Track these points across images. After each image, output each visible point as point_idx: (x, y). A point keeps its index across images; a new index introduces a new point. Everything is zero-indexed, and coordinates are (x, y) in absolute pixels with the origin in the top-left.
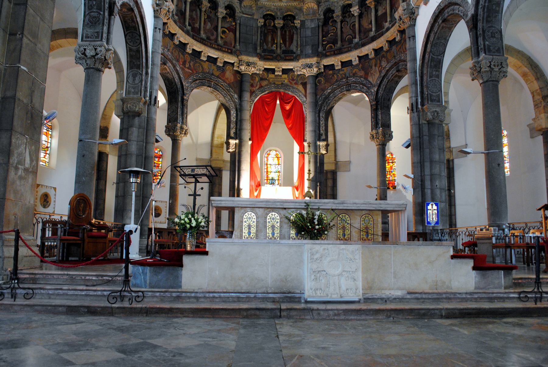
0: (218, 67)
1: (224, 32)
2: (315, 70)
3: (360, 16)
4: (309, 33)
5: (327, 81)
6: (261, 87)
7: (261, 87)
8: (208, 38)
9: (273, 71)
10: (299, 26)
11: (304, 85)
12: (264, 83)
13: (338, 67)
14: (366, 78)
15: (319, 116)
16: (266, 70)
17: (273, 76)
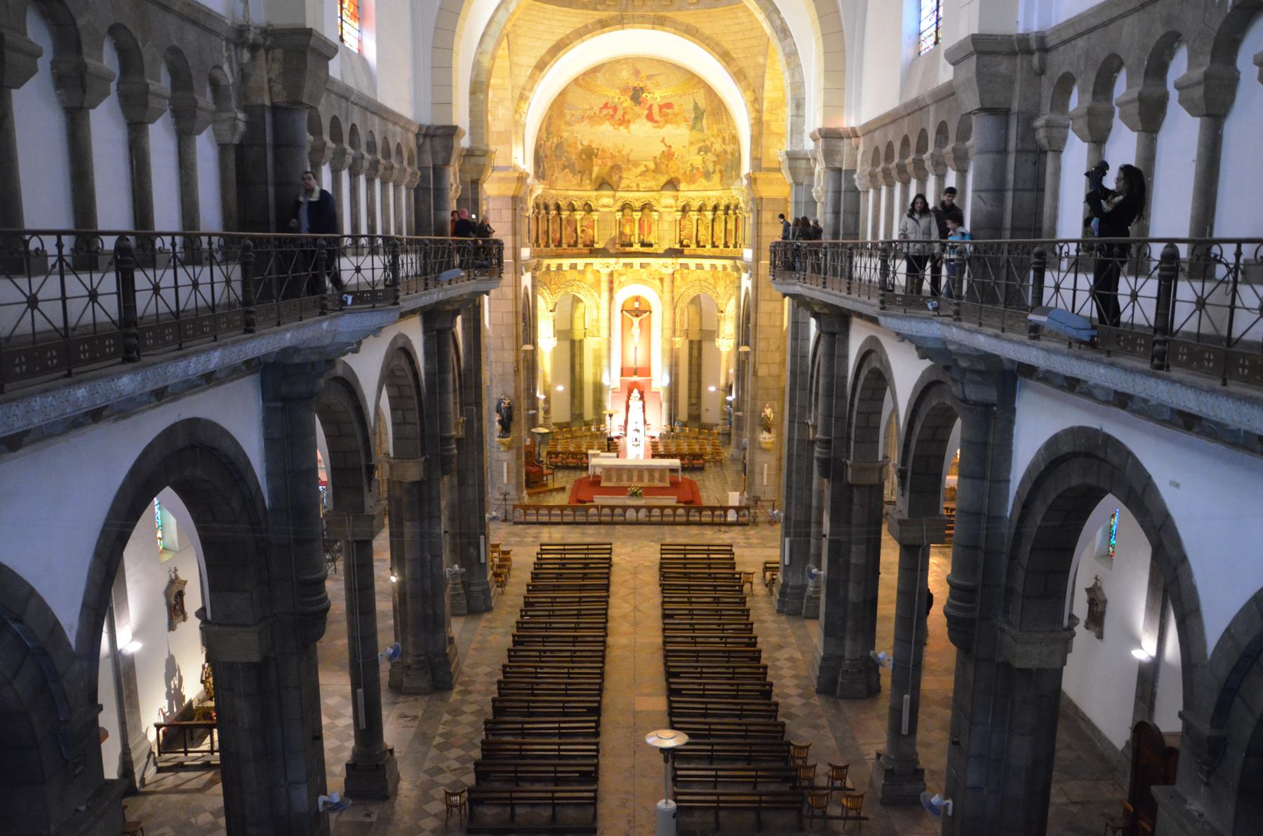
0: (580, 272)
1: (583, 231)
2: (670, 271)
3: (713, 220)
4: (666, 226)
5: (683, 278)
6: (620, 282)
7: (620, 282)
8: (569, 246)
9: (631, 265)
10: (656, 218)
11: (661, 280)
12: (623, 279)
13: (693, 267)
14: (715, 288)
15: (675, 313)
16: (625, 265)
17: (630, 270)
